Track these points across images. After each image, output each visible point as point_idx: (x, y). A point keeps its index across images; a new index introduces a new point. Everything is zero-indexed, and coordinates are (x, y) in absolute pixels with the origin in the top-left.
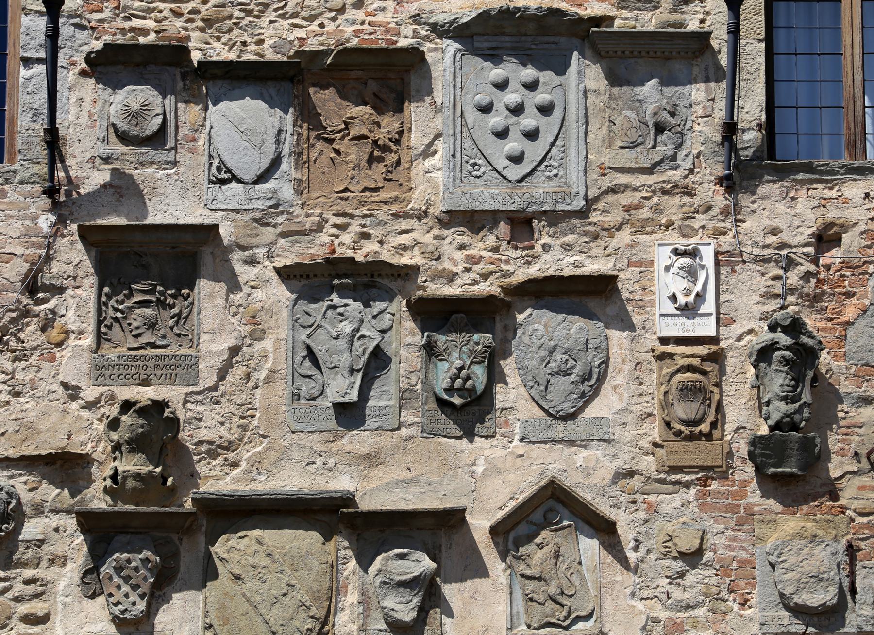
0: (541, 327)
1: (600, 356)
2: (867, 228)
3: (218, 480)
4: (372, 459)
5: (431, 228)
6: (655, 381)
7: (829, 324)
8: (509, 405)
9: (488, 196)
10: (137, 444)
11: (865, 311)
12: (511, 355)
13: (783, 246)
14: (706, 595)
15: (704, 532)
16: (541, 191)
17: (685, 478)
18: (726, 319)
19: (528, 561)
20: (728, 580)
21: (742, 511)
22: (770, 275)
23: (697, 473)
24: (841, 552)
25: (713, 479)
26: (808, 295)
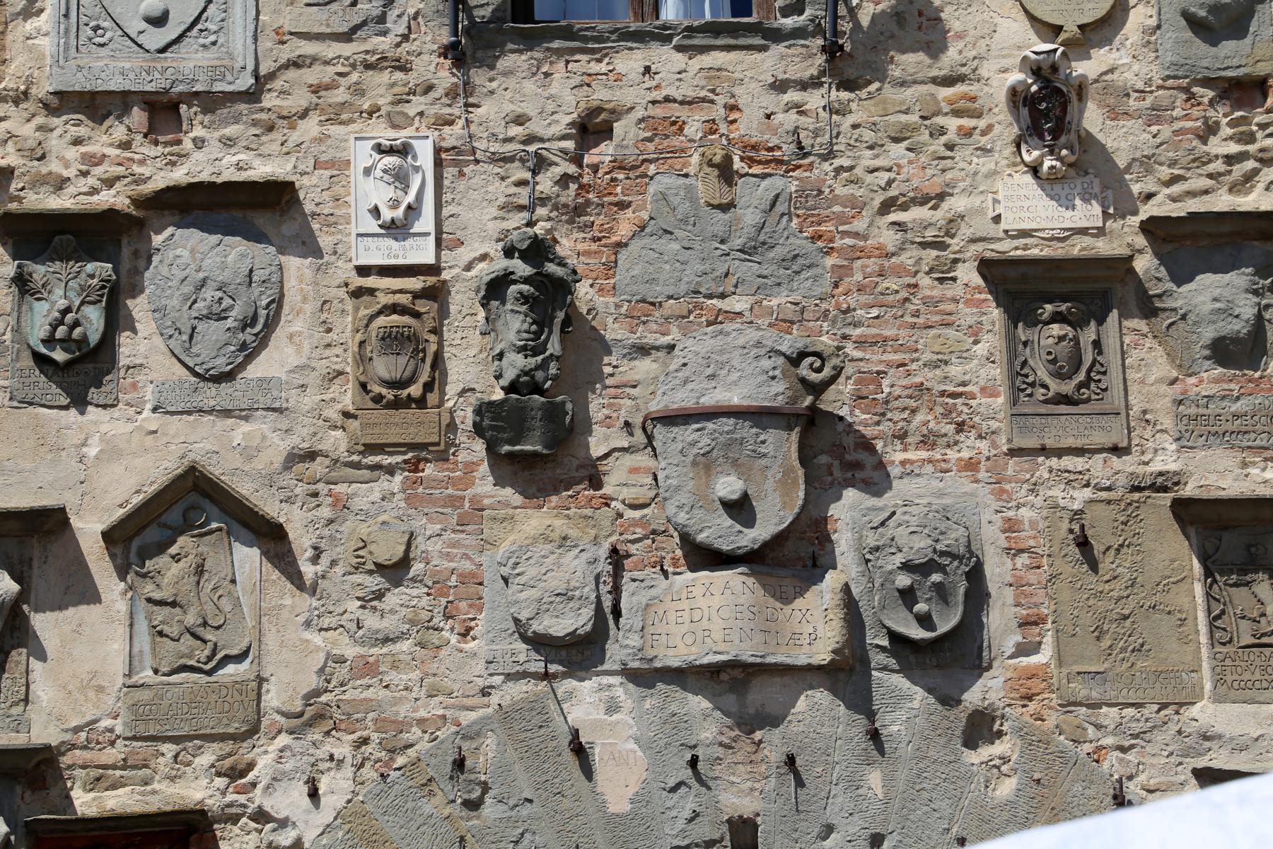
0: (186, 253)
1: (269, 292)
2: (646, 114)
5: (34, 116)
6: (350, 326)
7: (594, 247)
8: (138, 362)
9: (115, 70)
11: (643, 228)
12: (142, 291)
13: (531, 139)
14: (413, 622)
15: (412, 534)
16: (191, 65)
17: (387, 460)
18: (450, 240)
19: (158, 579)
20: (443, 601)
21: (467, 505)
22: (513, 179)
23: (404, 453)
24: (603, 560)
25: (427, 461)
26: (565, 206)
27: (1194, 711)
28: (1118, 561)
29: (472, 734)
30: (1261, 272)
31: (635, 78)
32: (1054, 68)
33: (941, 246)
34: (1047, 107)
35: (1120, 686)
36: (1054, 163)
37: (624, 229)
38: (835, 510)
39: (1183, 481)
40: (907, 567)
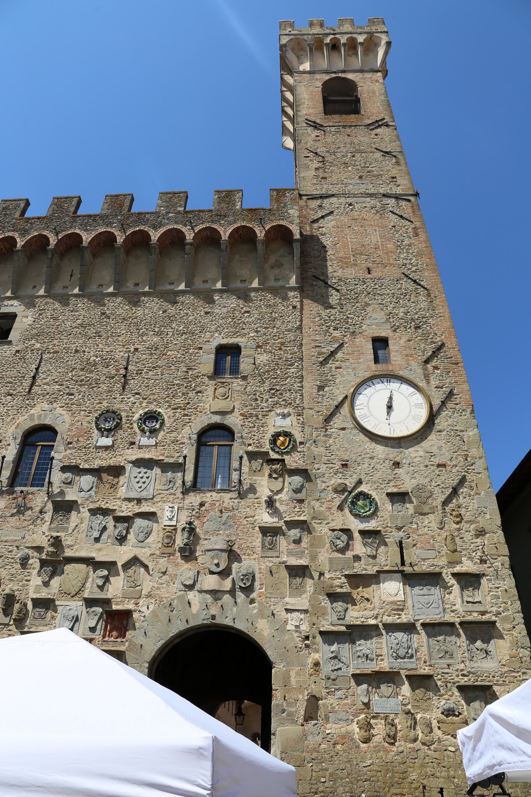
3: (68, 553)
4: (100, 550)
10: (52, 545)
13: (192, 506)
16: (144, 494)
17: (165, 555)
29: (173, 600)
30: (301, 529)
31: (209, 497)
33: (253, 524)
34: (270, 503)
37: (205, 520)
38: (233, 566)
40: (242, 575)
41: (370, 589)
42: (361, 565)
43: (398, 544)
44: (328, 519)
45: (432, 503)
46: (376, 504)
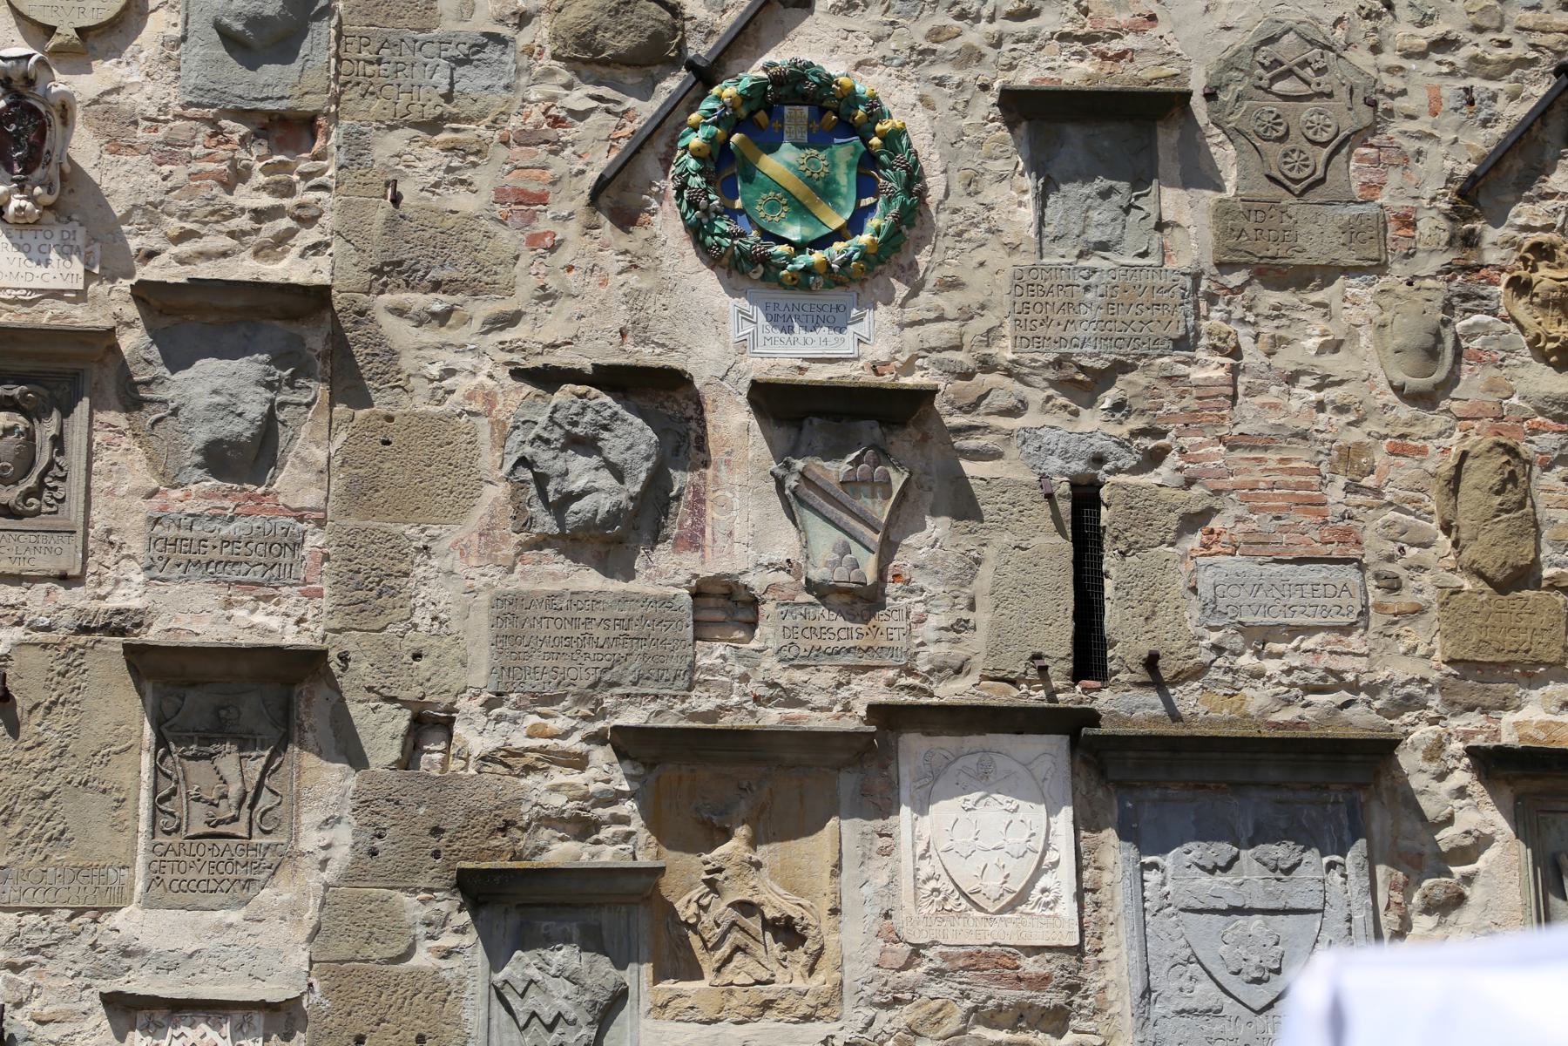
27: (117, 919)
28: (46, 723)
30: (278, 360)
32: (30, 82)
35: (25, 885)
36: (23, 203)
39: (146, 623)
41: (815, 849)
42: (752, 659)
43: (1065, 506)
44: (510, 290)
45: (1372, 187)
46: (913, 178)
